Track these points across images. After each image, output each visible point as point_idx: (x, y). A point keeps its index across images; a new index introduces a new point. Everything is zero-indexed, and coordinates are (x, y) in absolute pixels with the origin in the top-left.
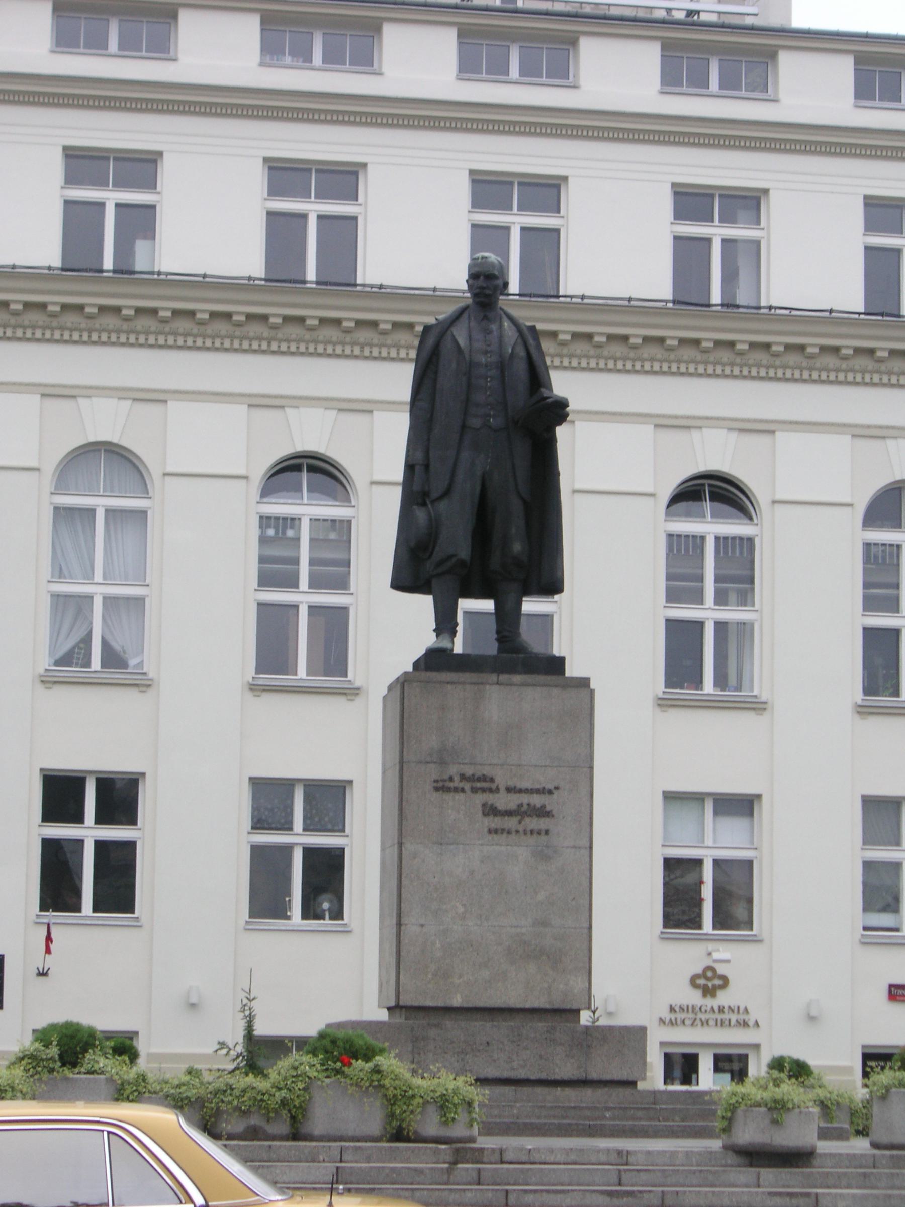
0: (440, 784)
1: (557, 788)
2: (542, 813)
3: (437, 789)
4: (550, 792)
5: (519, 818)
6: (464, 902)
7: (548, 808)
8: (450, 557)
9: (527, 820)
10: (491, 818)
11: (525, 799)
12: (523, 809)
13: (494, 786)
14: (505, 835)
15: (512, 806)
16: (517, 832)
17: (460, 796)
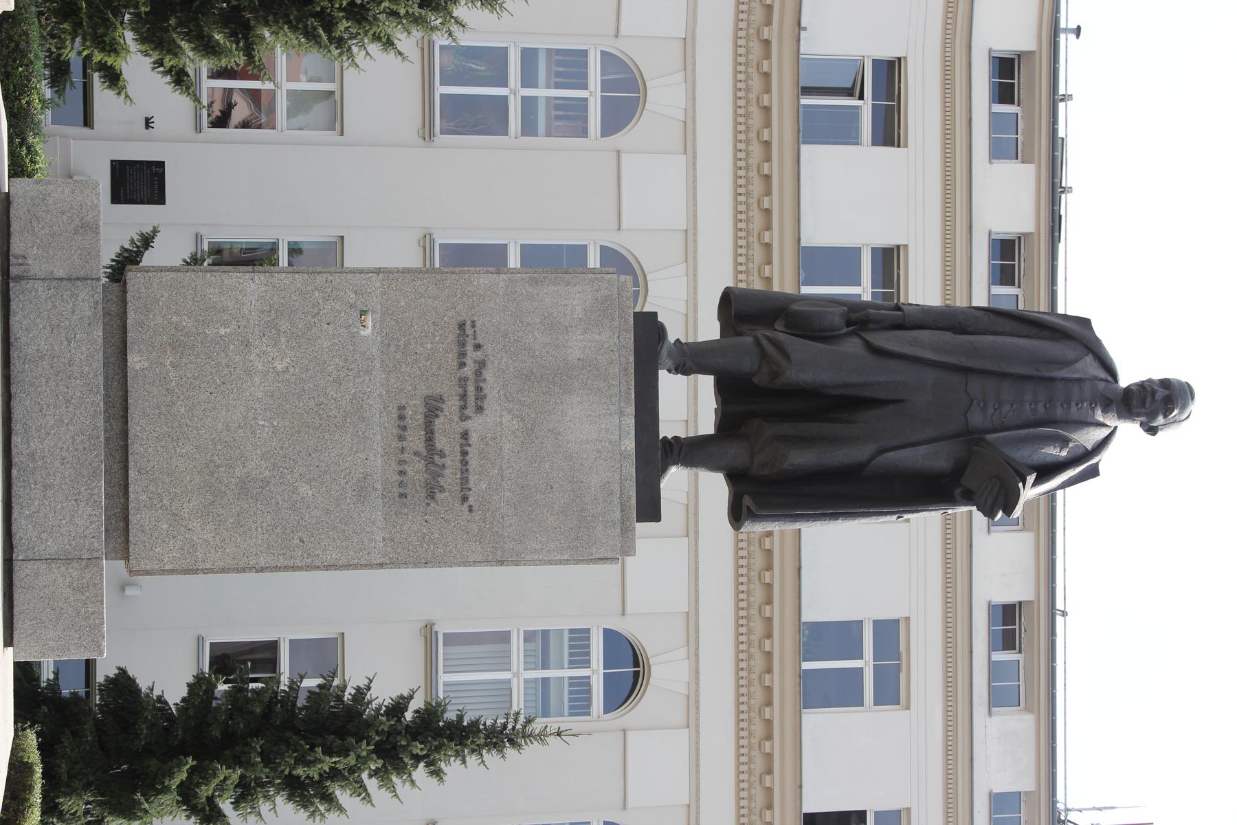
0: (469, 331)
1: (471, 509)
2: (432, 492)
3: (462, 326)
4: (465, 499)
5: (423, 451)
6: (291, 370)
7: (440, 496)
8: (786, 356)
9: (421, 465)
10: (422, 409)
11: (451, 460)
12: (436, 458)
13: (469, 411)
14: (396, 431)
15: (441, 442)
16: (403, 450)
17: (452, 359)
